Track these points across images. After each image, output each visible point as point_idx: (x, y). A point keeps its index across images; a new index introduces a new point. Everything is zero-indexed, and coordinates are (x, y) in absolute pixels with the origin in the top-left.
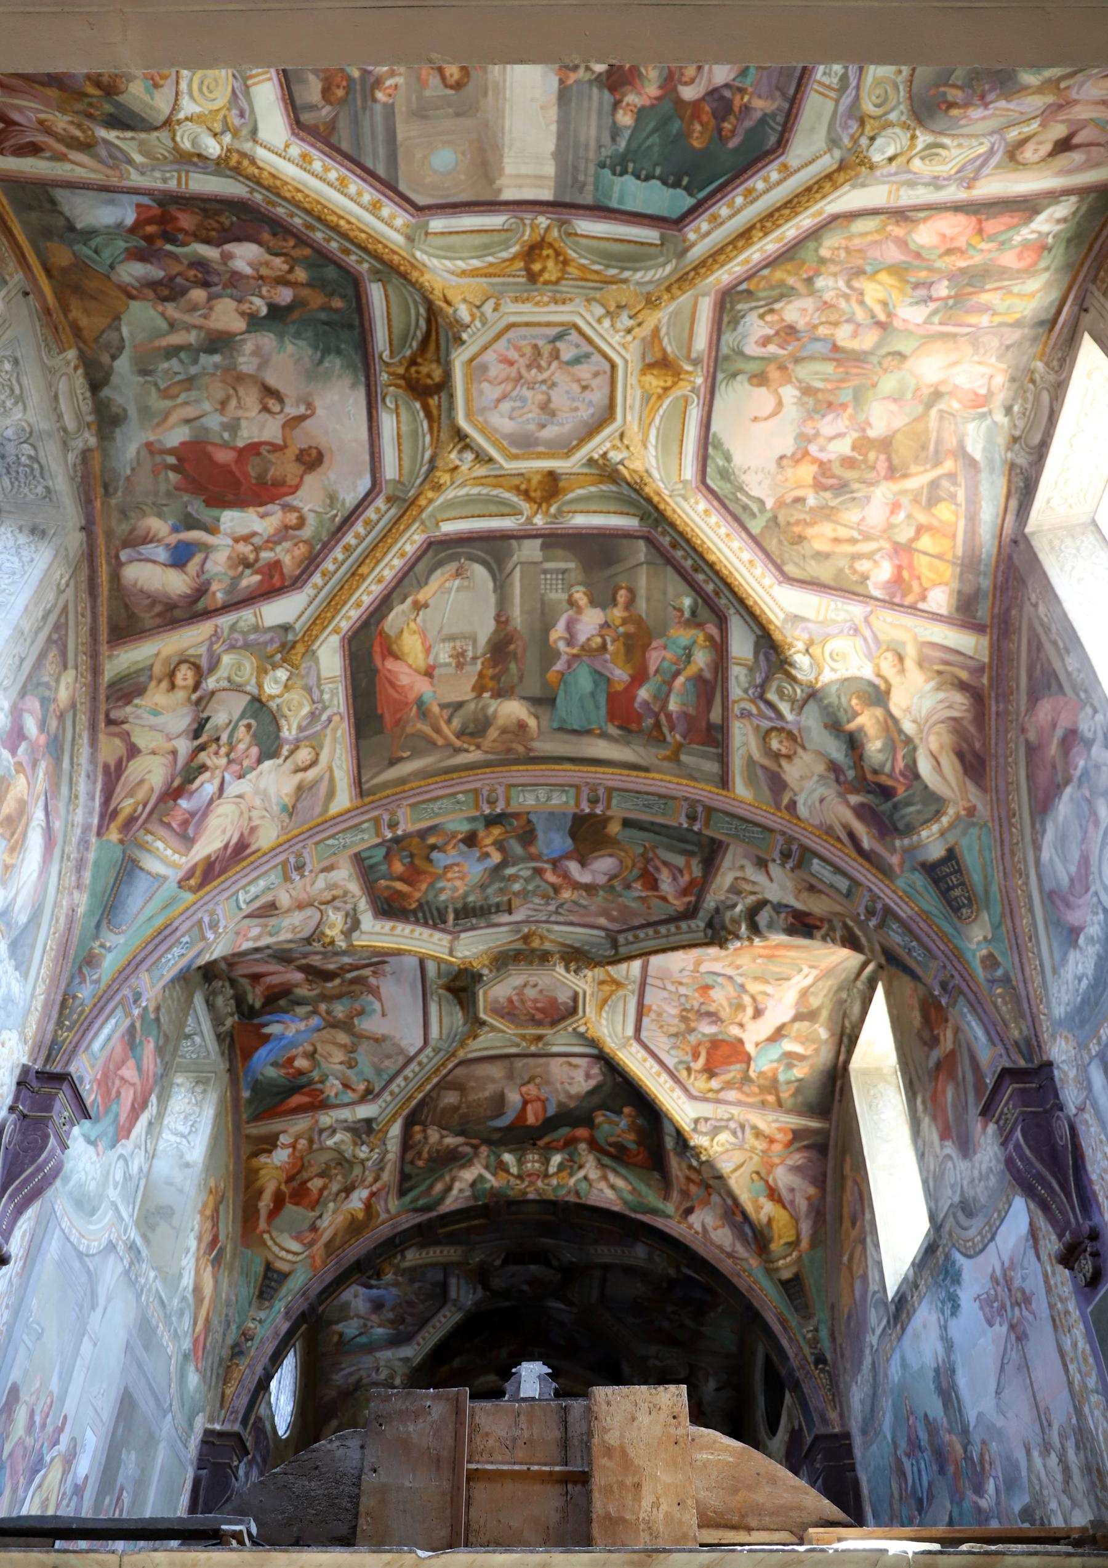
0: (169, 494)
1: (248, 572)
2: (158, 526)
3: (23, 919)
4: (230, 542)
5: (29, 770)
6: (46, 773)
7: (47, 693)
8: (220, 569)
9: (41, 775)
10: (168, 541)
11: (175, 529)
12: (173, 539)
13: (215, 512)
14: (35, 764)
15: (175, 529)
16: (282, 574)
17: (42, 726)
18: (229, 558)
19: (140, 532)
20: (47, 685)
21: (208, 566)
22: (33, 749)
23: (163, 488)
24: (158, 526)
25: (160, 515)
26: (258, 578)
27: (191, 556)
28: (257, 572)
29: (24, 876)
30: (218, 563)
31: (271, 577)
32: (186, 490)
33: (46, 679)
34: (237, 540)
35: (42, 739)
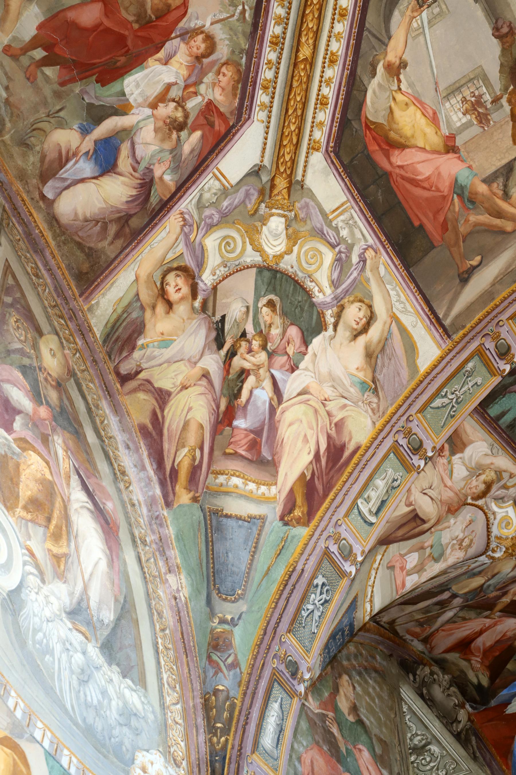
0: (58, 95)
1: (184, 134)
2: (66, 138)
3: (108, 616)
4: (148, 111)
5: (38, 445)
6: (67, 449)
7: (26, 361)
8: (153, 148)
9: (61, 452)
10: (84, 149)
11: (85, 132)
12: (88, 144)
13: (114, 87)
14: (45, 440)
15: (85, 132)
16: (221, 115)
17: (37, 396)
18: (156, 130)
19: (52, 155)
20: (22, 352)
21: (139, 153)
22: (34, 422)
23: (47, 91)
24: (66, 138)
25: (62, 125)
26: (198, 134)
27: (117, 151)
28: (193, 130)
29: (88, 567)
30: (148, 142)
31: (211, 125)
32: (72, 80)
33: (17, 346)
34: (154, 106)
35: (43, 412)
